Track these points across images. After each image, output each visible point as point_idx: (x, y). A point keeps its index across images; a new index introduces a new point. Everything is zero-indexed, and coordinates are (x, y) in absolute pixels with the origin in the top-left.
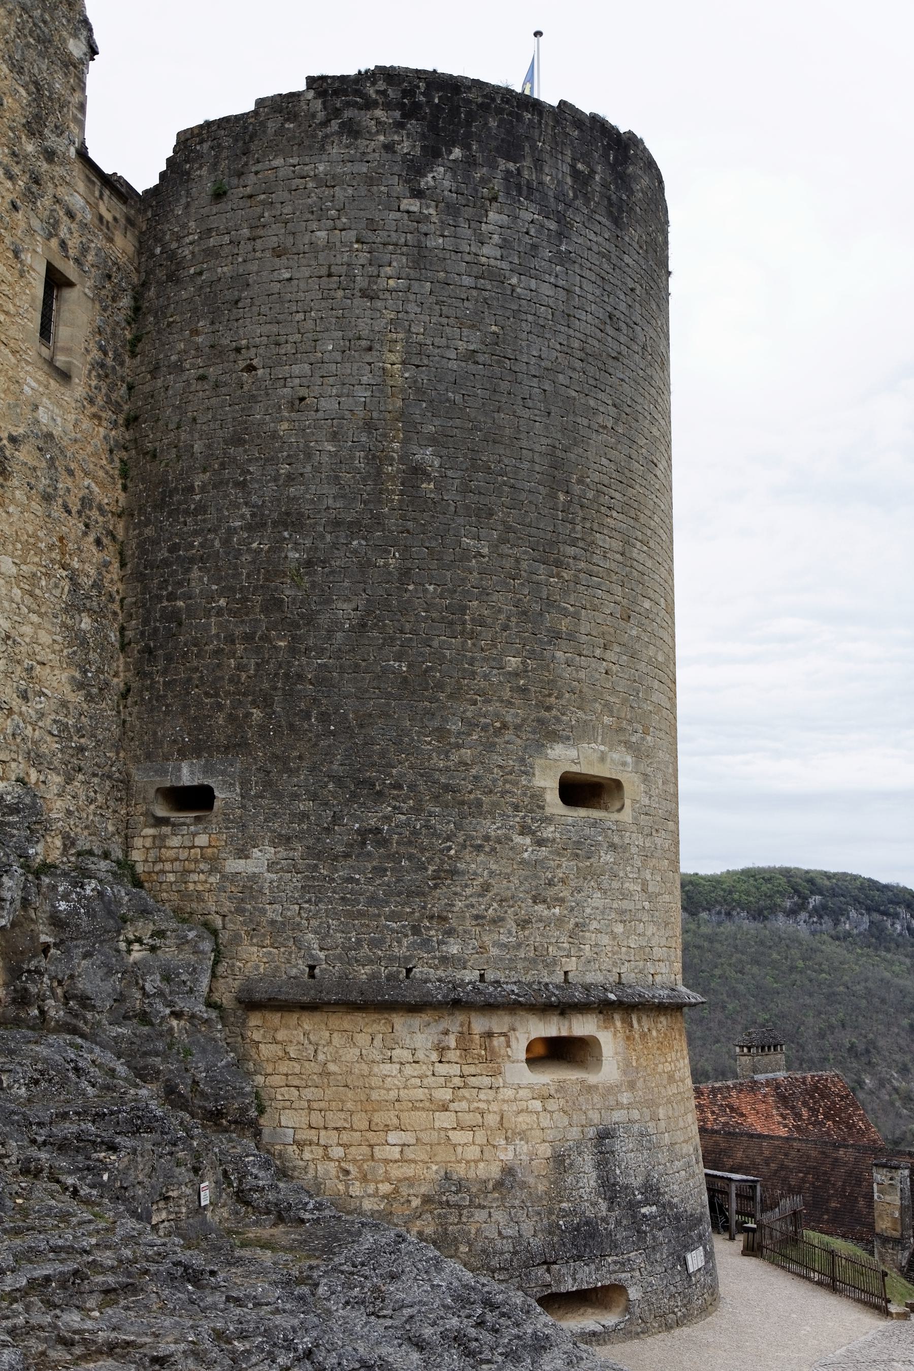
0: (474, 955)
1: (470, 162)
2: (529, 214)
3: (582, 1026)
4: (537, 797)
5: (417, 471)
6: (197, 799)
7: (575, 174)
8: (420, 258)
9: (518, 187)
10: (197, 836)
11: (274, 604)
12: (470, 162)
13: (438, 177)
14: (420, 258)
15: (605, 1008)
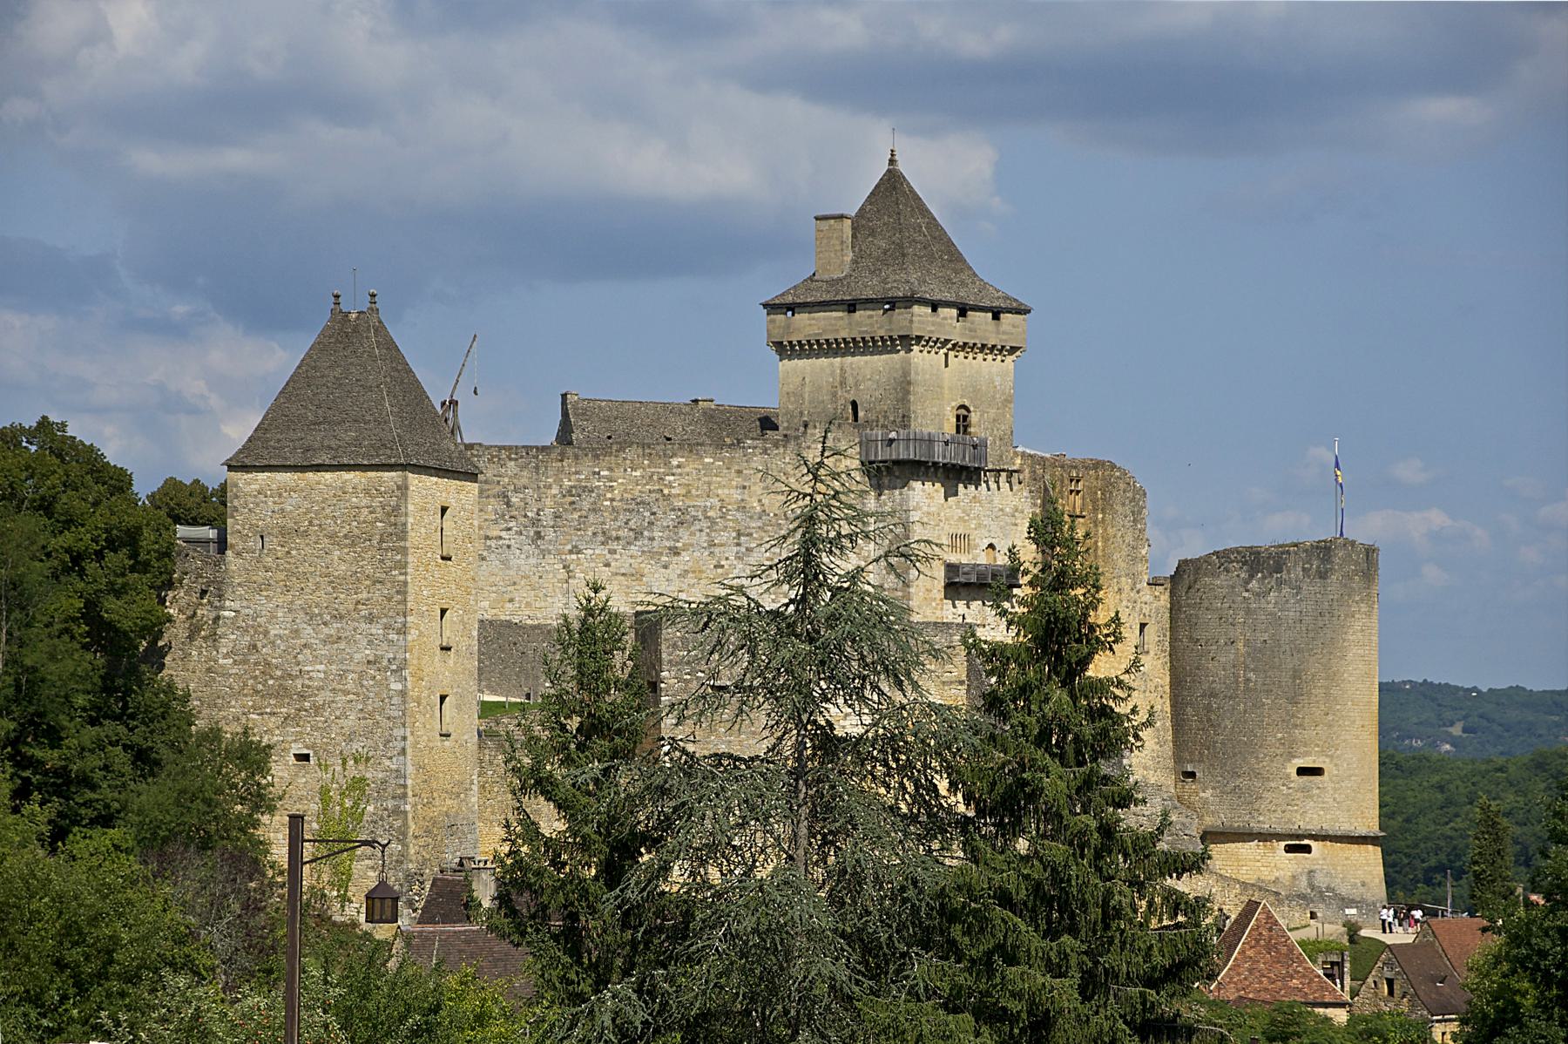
0: (1265, 823)
1: (1264, 578)
2: (1286, 590)
3: (1306, 842)
4: (1288, 776)
5: (1248, 680)
6: (1192, 775)
7: (1304, 569)
8: (1248, 611)
9: (1280, 583)
10: (1190, 786)
11: (1209, 720)
12: (1264, 578)
13: (1254, 584)
14: (1248, 611)
15: (1315, 837)
